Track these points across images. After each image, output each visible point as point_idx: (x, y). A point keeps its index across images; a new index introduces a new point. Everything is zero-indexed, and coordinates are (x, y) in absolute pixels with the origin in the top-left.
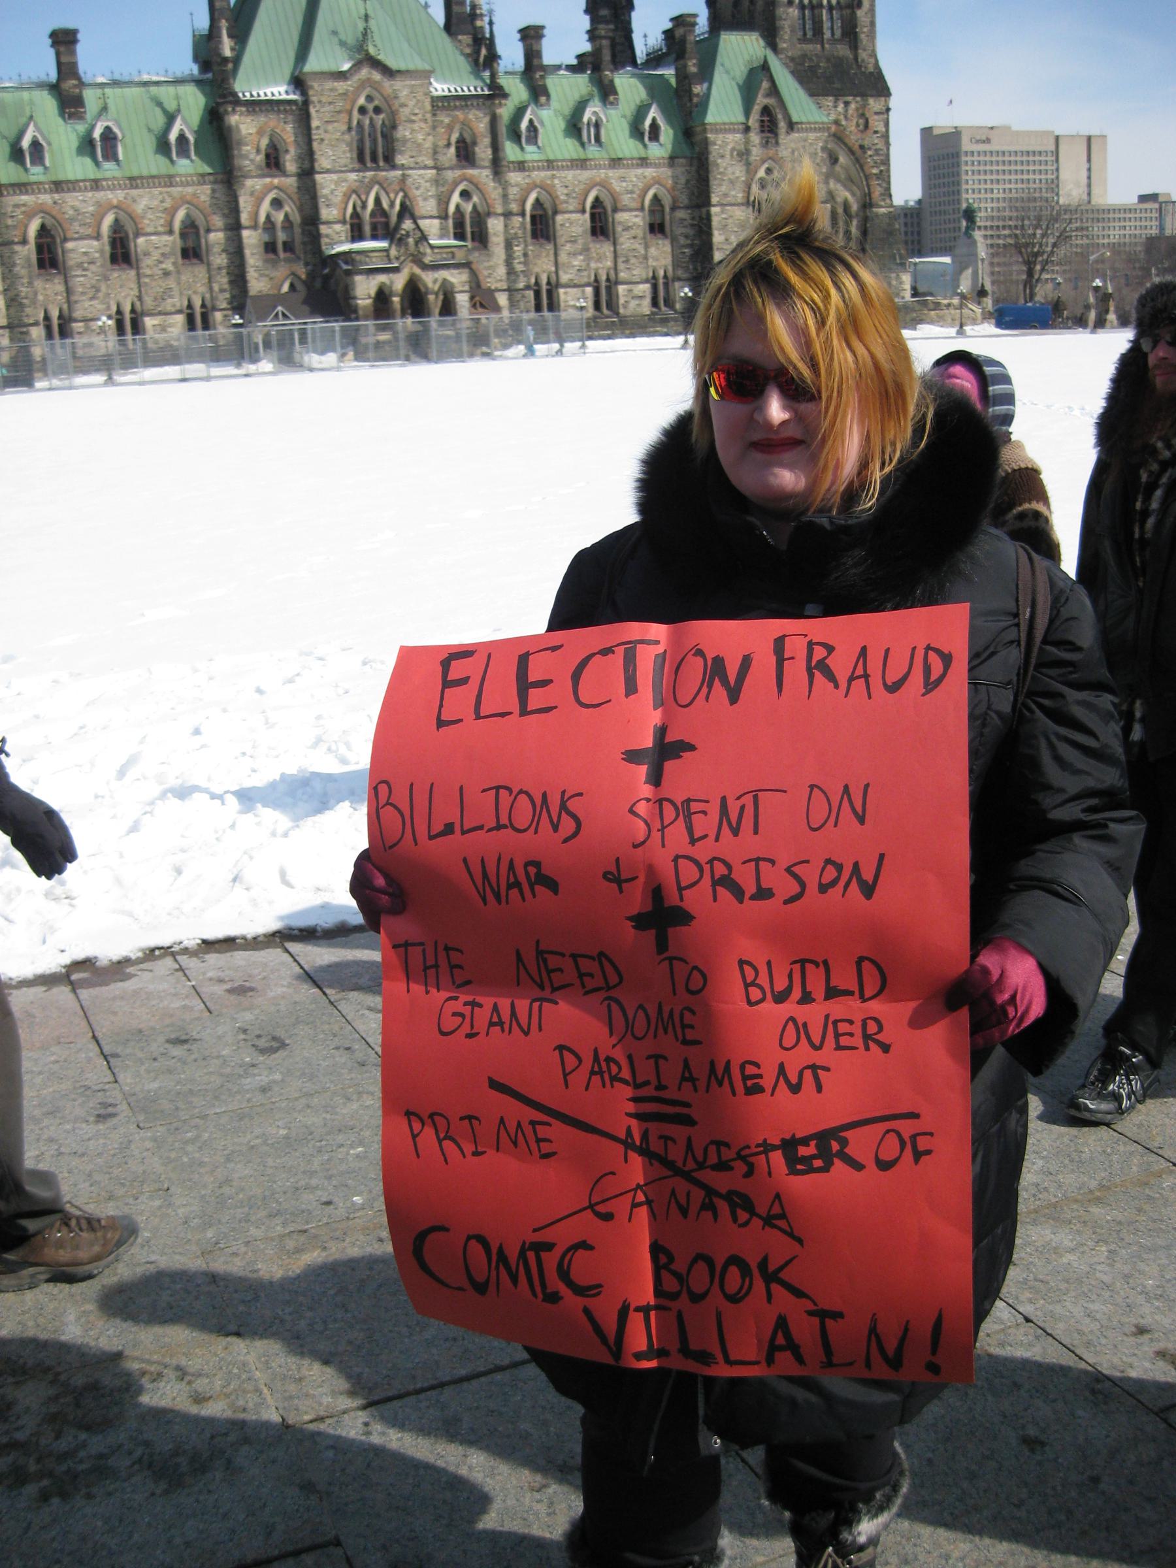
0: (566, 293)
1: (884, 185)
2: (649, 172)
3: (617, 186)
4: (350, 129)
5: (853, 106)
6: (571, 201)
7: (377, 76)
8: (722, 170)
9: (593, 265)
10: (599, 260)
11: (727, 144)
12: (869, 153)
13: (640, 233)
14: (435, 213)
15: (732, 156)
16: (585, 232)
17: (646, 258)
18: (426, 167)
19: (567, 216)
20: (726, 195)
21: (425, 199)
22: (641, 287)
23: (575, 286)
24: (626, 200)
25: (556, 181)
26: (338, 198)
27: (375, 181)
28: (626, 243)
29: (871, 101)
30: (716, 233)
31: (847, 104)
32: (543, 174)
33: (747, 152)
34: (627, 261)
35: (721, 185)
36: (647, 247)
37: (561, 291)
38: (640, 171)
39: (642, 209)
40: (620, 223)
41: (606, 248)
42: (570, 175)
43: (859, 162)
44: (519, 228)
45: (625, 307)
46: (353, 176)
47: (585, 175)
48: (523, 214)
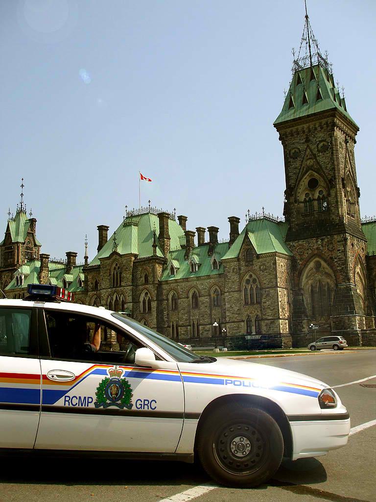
0: (181, 329)
1: (344, 274)
2: (212, 281)
3: (200, 287)
4: (110, 275)
5: (326, 240)
6: (183, 294)
7: (118, 257)
8: (229, 278)
9: (191, 318)
10: (194, 315)
11: (231, 267)
12: (335, 260)
13: (208, 305)
14: (131, 301)
15: (233, 271)
16: (189, 305)
17: (211, 315)
18: (129, 286)
19: (182, 300)
20: (231, 288)
21: (129, 296)
22: (208, 326)
23: (184, 326)
24: (203, 292)
25: (179, 287)
26: (105, 298)
27: (115, 292)
28: (202, 307)
29: (335, 237)
30: (227, 303)
31: (322, 240)
32: (174, 285)
33: (240, 269)
34: (203, 316)
35: (228, 284)
36: (211, 310)
37: (179, 328)
38: (208, 281)
39: (210, 295)
40: (201, 301)
41: (196, 311)
42: (183, 284)
43: (331, 266)
44: (166, 305)
45: (202, 335)
46: (110, 290)
47: (189, 283)
48: (167, 300)
